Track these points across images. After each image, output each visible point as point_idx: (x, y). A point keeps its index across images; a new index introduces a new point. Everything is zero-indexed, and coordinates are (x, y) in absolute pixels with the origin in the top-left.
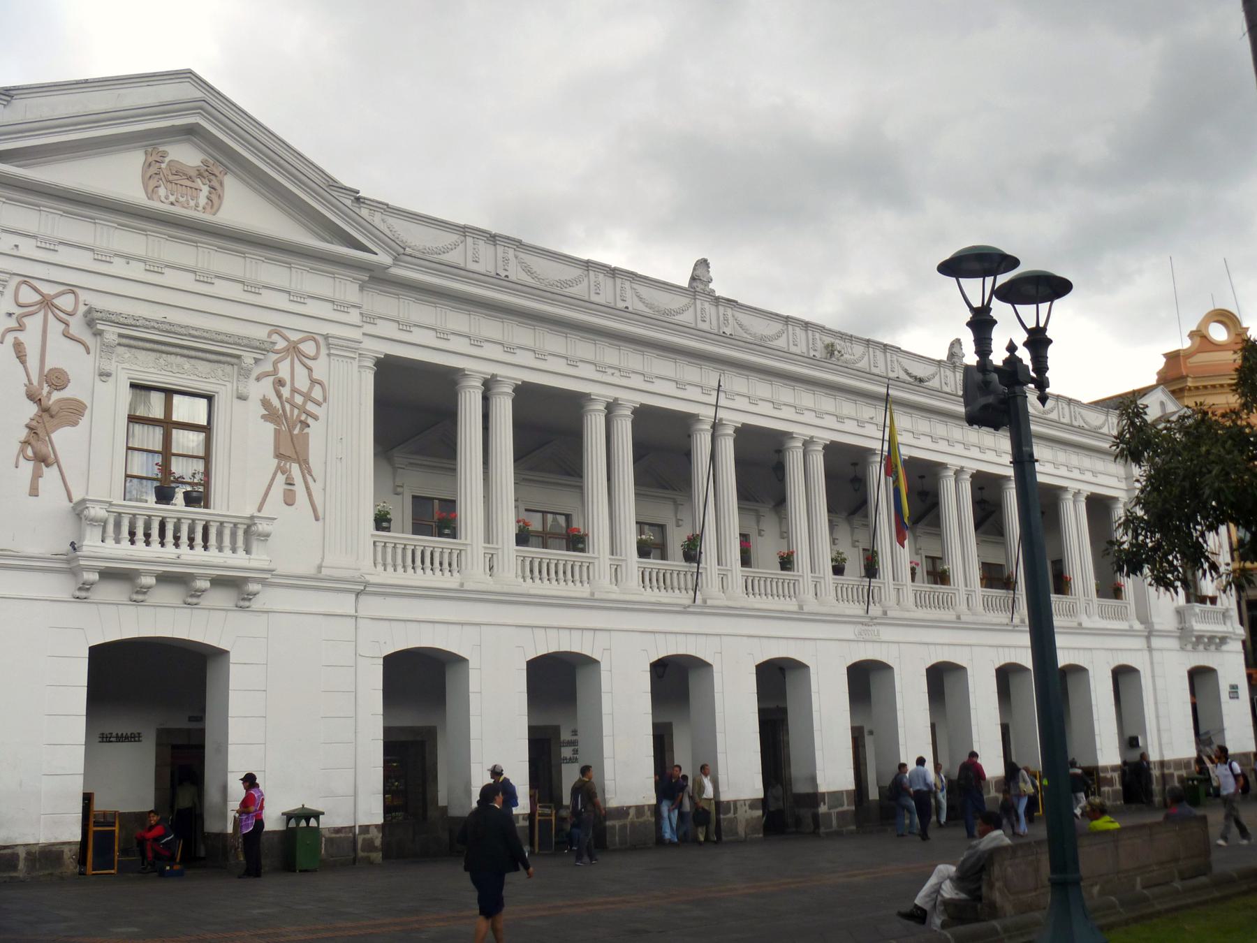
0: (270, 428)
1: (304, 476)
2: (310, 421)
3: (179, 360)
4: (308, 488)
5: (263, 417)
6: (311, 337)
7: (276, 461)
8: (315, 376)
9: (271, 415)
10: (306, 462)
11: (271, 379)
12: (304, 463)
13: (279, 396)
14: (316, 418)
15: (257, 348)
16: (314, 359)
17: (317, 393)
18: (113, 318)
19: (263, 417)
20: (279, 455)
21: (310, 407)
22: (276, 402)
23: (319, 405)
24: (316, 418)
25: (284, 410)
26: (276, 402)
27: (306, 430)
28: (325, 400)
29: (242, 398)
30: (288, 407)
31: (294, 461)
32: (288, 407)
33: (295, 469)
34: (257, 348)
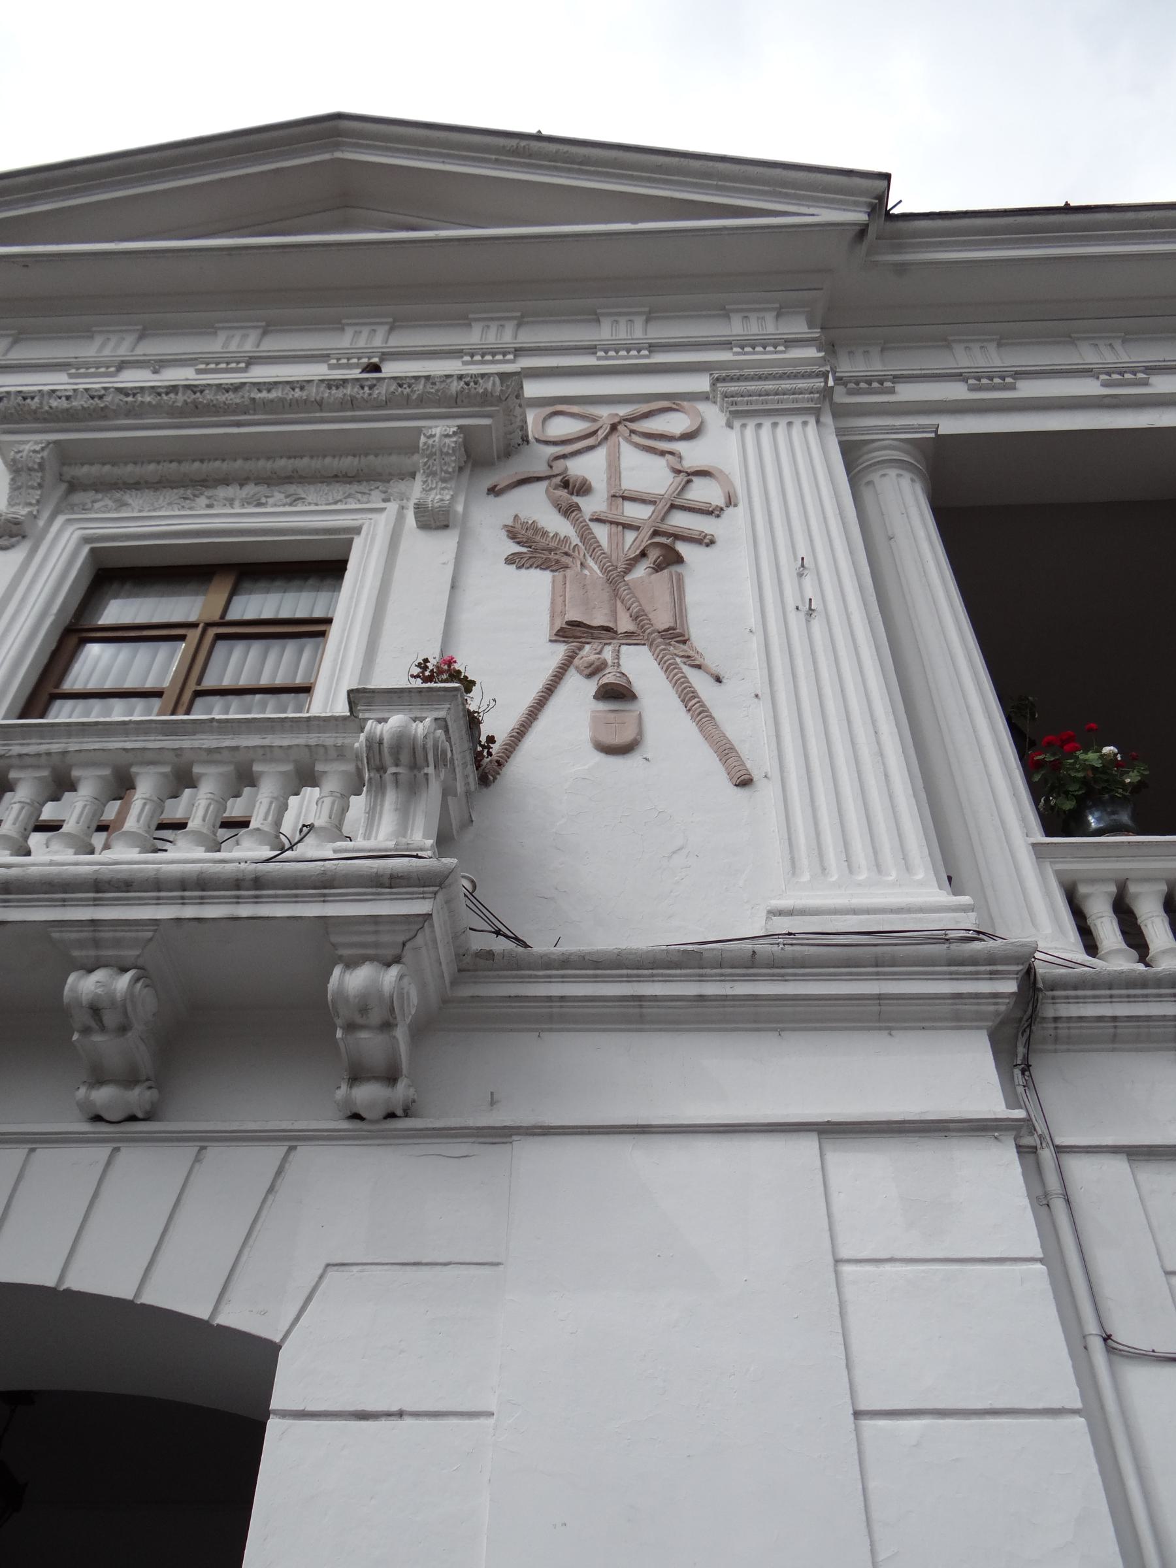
0: (540, 581)
1: (669, 669)
2: (682, 548)
3: (250, 489)
4: (688, 697)
5: (511, 560)
6: (673, 402)
7: (560, 651)
8: (690, 463)
9: (533, 550)
10: (676, 635)
11: (543, 485)
12: (673, 639)
13: (569, 511)
14: (707, 541)
15: (457, 400)
16: (688, 436)
17: (703, 492)
18: (34, 404)
19: (511, 560)
20: (572, 632)
21: (681, 521)
22: (556, 525)
23: (712, 512)
24: (707, 541)
25: (586, 535)
26: (556, 525)
27: (675, 569)
28: (731, 501)
29: (434, 520)
30: (601, 533)
31: (631, 638)
32: (601, 533)
33: (638, 665)
34: (457, 400)
